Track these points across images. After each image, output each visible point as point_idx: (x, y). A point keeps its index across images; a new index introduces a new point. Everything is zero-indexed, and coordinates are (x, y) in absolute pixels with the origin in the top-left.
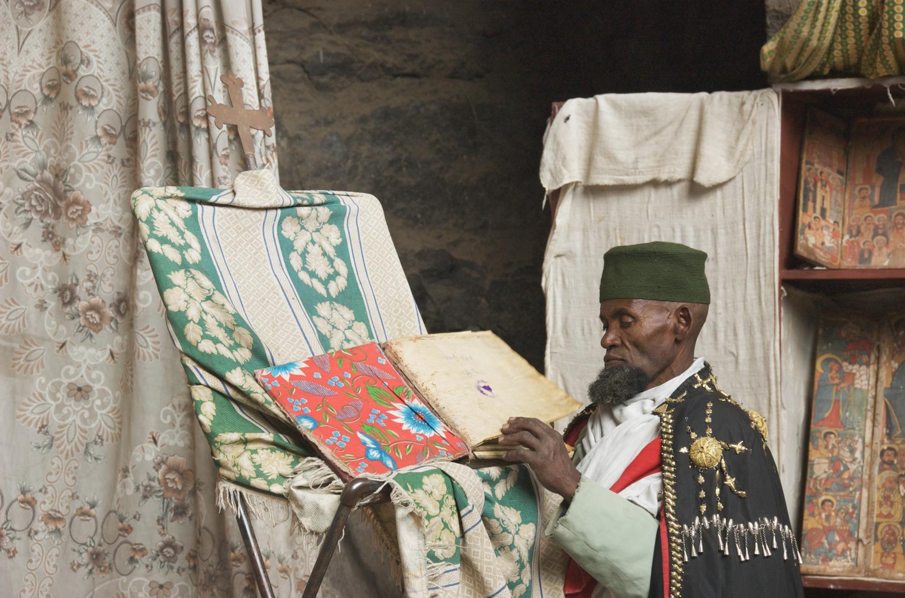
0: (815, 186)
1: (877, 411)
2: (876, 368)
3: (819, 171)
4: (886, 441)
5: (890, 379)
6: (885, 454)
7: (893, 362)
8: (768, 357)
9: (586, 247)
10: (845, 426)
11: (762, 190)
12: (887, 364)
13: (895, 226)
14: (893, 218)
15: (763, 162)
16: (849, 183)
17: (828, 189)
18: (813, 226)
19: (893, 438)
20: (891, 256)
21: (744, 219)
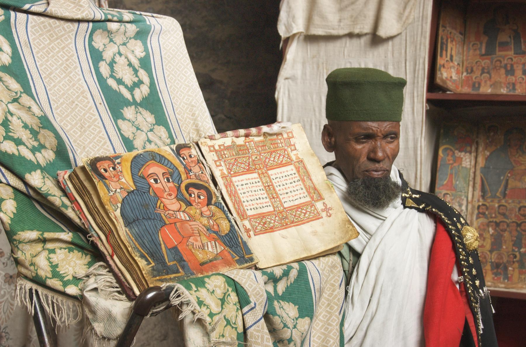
0: (447, 41)
1: (476, 181)
2: (475, 154)
3: (449, 32)
4: (481, 200)
5: (484, 162)
6: (480, 208)
7: (486, 152)
8: (417, 147)
9: (304, 74)
10: (456, 190)
11: (419, 42)
12: (483, 153)
13: (495, 68)
14: (494, 63)
15: (420, 23)
16: (466, 40)
17: (454, 43)
18: (446, 66)
19: (485, 198)
20: (492, 86)
21: (406, 60)
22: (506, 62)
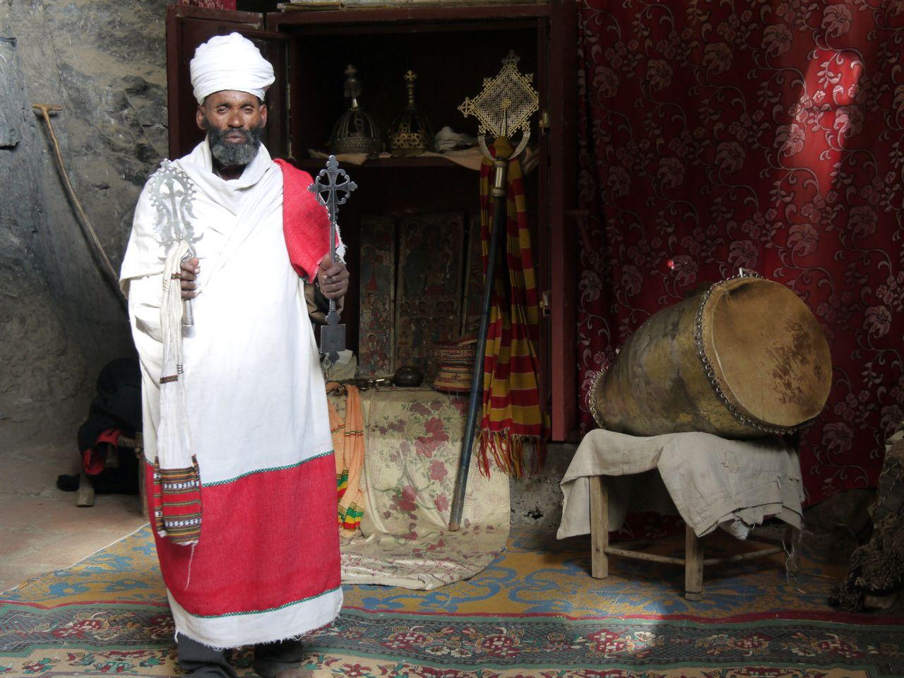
4: (404, 298)
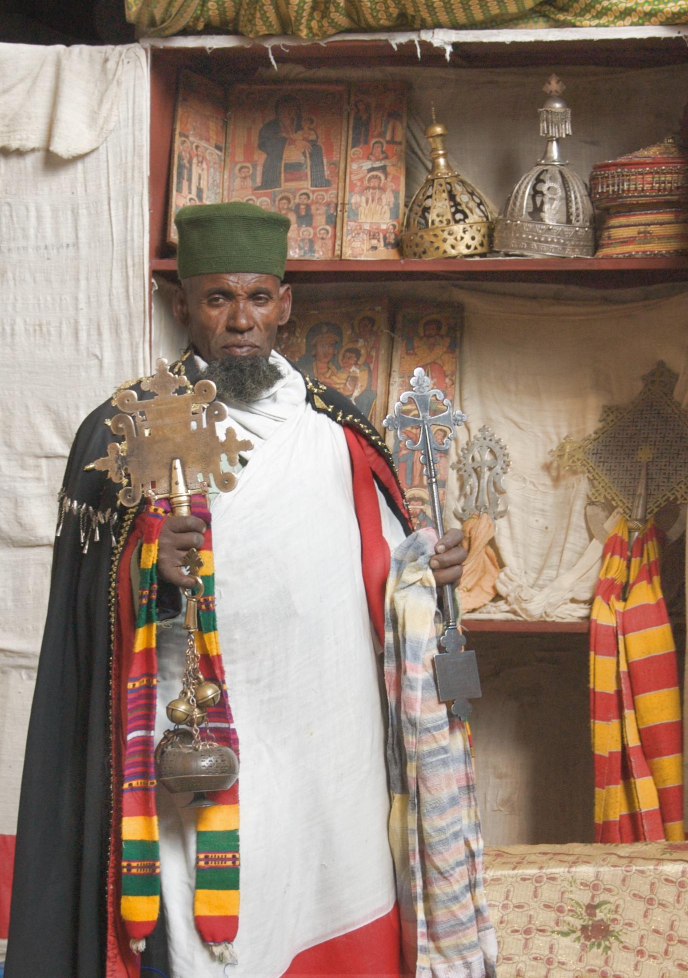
0: (190, 162)
3: (195, 145)
8: (137, 361)
11: (130, 164)
14: (277, 203)
15: (130, 131)
17: (204, 166)
21: (109, 199)
22: (297, 201)
